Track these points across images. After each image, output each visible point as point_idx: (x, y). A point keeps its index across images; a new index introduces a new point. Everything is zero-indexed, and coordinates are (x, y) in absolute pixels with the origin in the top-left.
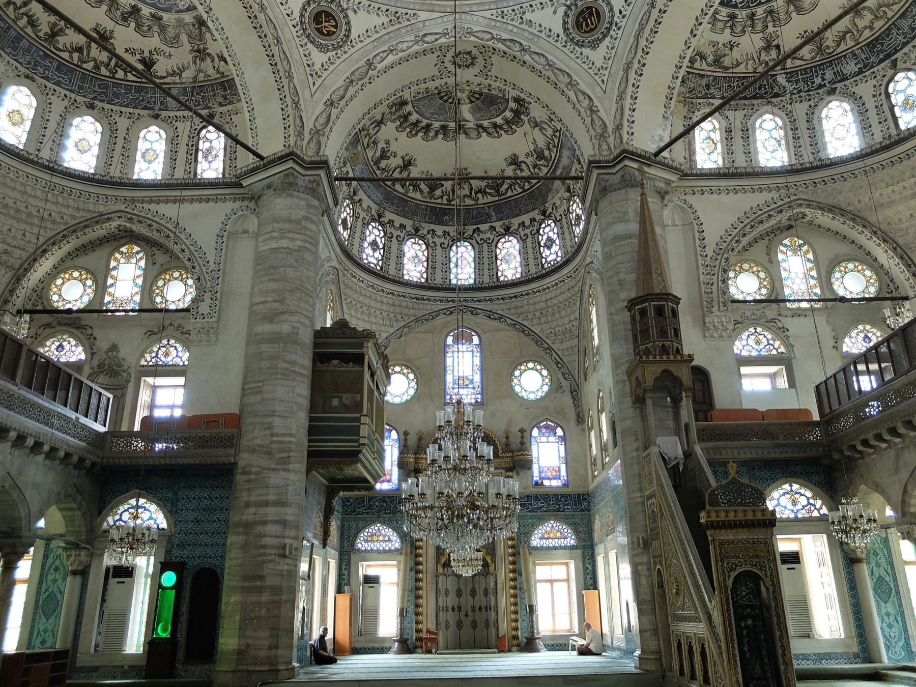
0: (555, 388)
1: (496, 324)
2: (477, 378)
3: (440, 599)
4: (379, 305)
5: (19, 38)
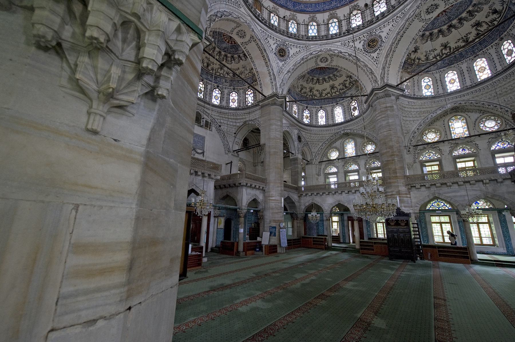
5: (461, 54)
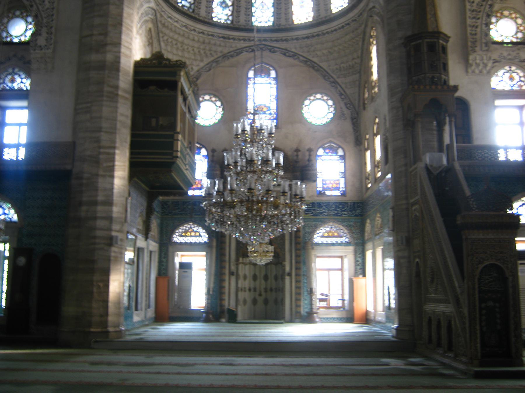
0: (338, 115)
1: (291, 60)
2: (273, 106)
3: (240, 282)
4: (191, 43)
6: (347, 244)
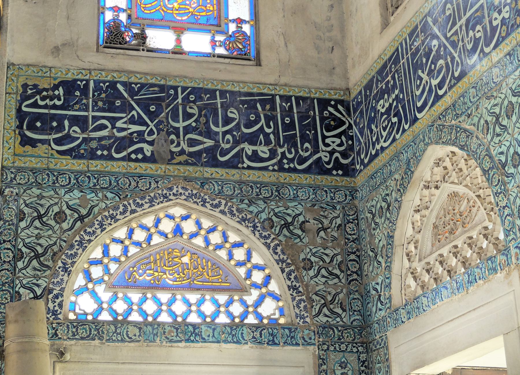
6: (268, 334)
